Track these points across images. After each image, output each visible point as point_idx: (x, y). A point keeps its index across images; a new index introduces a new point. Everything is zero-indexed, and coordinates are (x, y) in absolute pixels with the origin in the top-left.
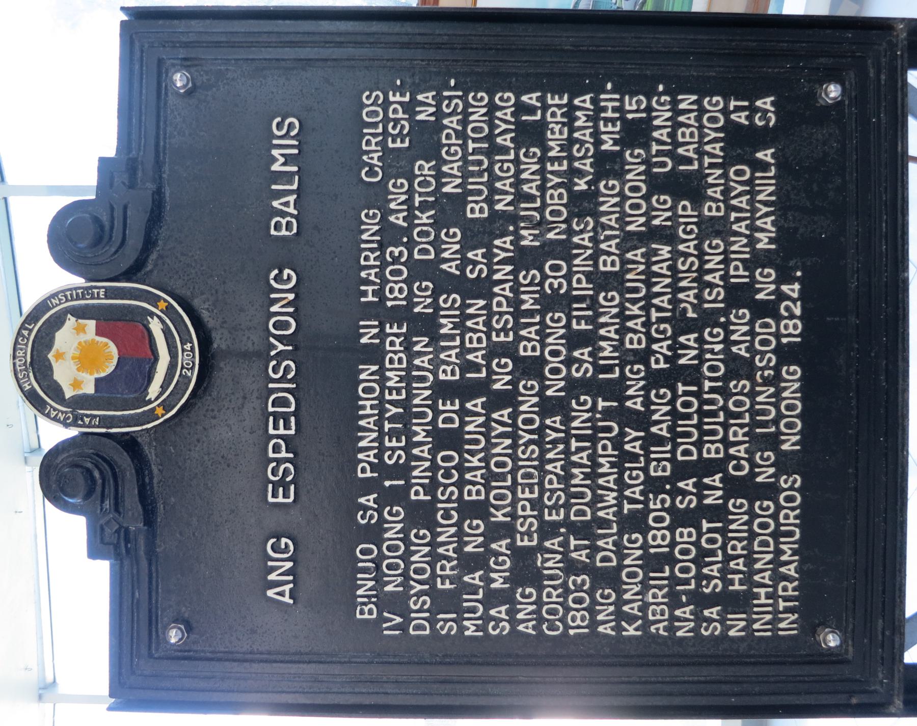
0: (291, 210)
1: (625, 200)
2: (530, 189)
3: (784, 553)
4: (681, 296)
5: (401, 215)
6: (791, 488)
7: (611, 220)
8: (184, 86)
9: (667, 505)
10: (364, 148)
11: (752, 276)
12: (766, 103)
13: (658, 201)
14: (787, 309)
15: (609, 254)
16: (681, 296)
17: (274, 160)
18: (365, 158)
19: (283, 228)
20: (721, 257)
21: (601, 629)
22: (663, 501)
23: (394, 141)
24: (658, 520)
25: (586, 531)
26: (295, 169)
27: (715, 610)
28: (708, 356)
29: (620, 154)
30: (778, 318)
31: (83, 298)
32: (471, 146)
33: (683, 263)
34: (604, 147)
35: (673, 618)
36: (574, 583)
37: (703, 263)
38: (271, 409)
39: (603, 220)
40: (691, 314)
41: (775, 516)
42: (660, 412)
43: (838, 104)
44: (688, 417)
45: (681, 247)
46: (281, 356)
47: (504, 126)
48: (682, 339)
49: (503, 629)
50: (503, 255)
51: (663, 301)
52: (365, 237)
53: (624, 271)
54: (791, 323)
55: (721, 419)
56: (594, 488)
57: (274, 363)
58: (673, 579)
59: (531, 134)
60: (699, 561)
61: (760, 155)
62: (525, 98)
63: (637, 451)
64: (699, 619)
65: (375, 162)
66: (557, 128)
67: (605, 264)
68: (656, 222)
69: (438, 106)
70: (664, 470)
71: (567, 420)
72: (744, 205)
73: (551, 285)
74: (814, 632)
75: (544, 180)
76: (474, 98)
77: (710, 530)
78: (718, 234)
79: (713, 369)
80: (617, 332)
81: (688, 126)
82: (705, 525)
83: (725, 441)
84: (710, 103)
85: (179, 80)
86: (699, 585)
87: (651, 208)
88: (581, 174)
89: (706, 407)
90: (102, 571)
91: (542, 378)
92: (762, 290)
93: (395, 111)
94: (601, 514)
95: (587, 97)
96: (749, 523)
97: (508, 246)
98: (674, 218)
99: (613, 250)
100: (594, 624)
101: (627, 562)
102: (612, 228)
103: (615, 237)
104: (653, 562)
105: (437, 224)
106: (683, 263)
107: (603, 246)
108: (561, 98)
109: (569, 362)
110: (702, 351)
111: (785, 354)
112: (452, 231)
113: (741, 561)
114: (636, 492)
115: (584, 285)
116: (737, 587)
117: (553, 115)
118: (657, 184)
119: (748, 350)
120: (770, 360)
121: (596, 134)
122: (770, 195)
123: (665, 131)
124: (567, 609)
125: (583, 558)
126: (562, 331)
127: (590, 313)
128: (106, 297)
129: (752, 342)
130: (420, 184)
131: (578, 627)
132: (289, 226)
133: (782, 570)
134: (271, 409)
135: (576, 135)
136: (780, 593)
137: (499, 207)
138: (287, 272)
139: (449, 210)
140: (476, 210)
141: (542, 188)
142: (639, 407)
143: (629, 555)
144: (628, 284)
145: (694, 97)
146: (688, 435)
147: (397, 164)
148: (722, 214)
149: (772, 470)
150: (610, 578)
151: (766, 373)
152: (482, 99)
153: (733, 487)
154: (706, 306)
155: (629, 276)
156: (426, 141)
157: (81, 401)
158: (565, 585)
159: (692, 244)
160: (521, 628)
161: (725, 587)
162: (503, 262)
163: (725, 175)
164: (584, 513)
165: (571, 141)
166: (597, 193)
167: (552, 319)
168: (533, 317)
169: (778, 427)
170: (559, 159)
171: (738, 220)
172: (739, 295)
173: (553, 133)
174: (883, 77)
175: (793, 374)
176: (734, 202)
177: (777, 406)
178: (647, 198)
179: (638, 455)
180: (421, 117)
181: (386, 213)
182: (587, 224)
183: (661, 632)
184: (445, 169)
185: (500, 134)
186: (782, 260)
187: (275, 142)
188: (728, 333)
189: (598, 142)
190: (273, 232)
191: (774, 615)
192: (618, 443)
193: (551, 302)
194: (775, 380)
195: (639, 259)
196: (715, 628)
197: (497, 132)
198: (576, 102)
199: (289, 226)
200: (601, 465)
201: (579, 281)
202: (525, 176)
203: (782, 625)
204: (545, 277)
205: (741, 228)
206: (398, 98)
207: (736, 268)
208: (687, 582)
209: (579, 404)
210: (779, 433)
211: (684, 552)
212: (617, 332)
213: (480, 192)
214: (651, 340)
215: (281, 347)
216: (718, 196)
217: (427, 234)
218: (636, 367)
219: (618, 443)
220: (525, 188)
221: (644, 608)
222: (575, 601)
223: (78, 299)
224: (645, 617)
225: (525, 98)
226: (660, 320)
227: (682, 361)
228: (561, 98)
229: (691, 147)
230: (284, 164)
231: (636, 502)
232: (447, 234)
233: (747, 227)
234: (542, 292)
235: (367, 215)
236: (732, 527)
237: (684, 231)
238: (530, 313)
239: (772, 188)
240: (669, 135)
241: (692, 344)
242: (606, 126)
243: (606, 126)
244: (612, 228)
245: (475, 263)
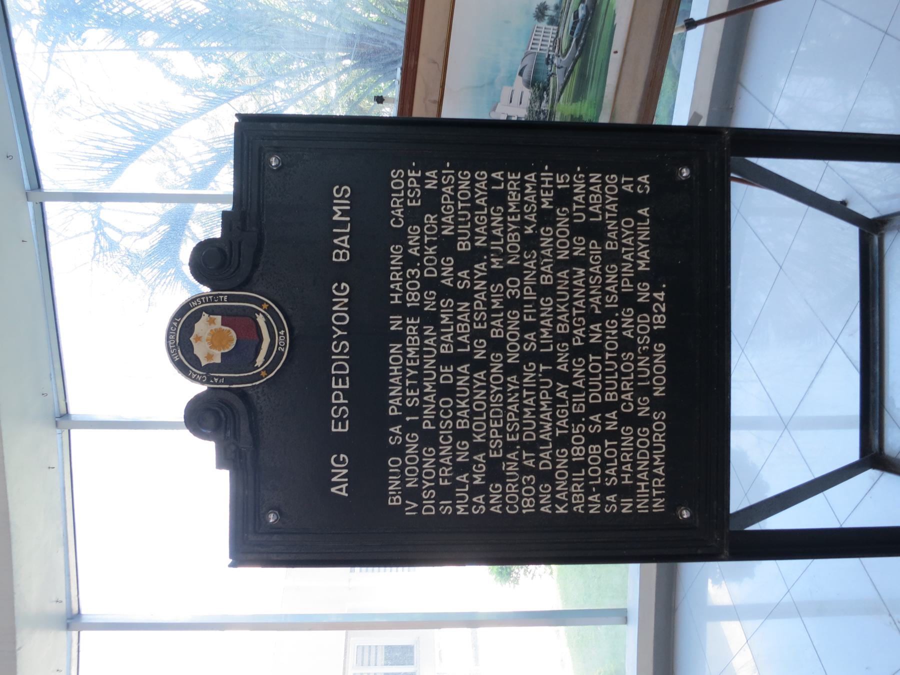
0: (346, 245)
1: (557, 241)
2: (497, 232)
3: (656, 460)
4: (591, 300)
5: (416, 249)
6: (660, 420)
7: (548, 252)
8: (276, 166)
9: (583, 431)
10: (392, 206)
11: (635, 288)
12: (644, 179)
13: (577, 240)
14: (657, 308)
15: (547, 274)
16: (591, 300)
17: (335, 213)
18: (393, 212)
19: (341, 256)
20: (615, 276)
21: (542, 509)
22: (581, 428)
23: (411, 202)
24: (578, 440)
25: (534, 447)
26: (348, 219)
27: (613, 496)
28: (608, 337)
29: (554, 210)
30: (651, 314)
31: (213, 302)
32: (460, 205)
33: (593, 280)
34: (543, 206)
35: (587, 502)
36: (526, 480)
37: (604, 279)
38: (333, 372)
39: (543, 252)
40: (597, 312)
41: (650, 438)
42: (579, 372)
43: (688, 180)
44: (596, 375)
45: (591, 269)
46: (340, 338)
47: (481, 193)
48: (592, 327)
49: (481, 510)
50: (480, 274)
51: (580, 303)
52: (393, 262)
53: (556, 284)
54: (659, 317)
55: (616, 377)
56: (538, 420)
57: (335, 343)
58: (587, 478)
59: (497, 198)
60: (603, 466)
61: (640, 212)
62: (493, 175)
63: (564, 397)
64: (603, 502)
65: (399, 215)
66: (514, 194)
67: (544, 280)
68: (576, 254)
69: (439, 179)
70: (581, 408)
71: (521, 378)
72: (630, 243)
73: (510, 293)
74: (675, 510)
75: (506, 227)
76: (462, 175)
77: (609, 446)
78: (613, 262)
79: (611, 345)
80: (551, 322)
81: (595, 193)
82: (607, 443)
83: (618, 390)
84: (609, 179)
85: (274, 161)
86: (603, 481)
87: (572, 245)
88: (529, 223)
89: (607, 370)
90: (224, 476)
91: (505, 352)
92: (642, 296)
93: (412, 183)
94: (542, 437)
95: (533, 175)
96: (634, 442)
97: (483, 268)
98: (587, 251)
99: (549, 271)
100: (538, 506)
101: (558, 467)
102: (548, 257)
103: (549, 263)
104: (574, 467)
105: (439, 254)
106: (593, 280)
107: (543, 269)
108: (516, 175)
109: (522, 341)
110: (604, 335)
111: (656, 336)
112: (448, 259)
113: (629, 465)
114: (563, 423)
115: (531, 293)
116: (627, 482)
117: (512, 186)
118: (576, 230)
119: (632, 333)
120: (646, 340)
121: (538, 198)
122: (646, 236)
123: (581, 196)
124: (521, 497)
125: (531, 465)
126: (517, 322)
127: (535, 311)
128: (228, 301)
129: (635, 329)
130: (427, 229)
131: (528, 508)
132: (344, 255)
133: (655, 471)
134: (333, 372)
135: (526, 198)
136: (654, 485)
137: (478, 244)
138: (343, 284)
139: (446, 246)
140: (463, 246)
141: (505, 232)
142: (565, 370)
143: (559, 462)
144: (559, 293)
145: (599, 175)
146: (596, 387)
147: (413, 216)
148: (616, 248)
149: (648, 409)
150: (547, 477)
151: (644, 348)
152: (467, 175)
153: (624, 419)
154: (607, 306)
155: (559, 288)
156: (432, 201)
157: (211, 368)
158: (520, 481)
159: (598, 267)
160: (492, 509)
161: (619, 482)
162: (481, 278)
163: (619, 224)
164: (531, 436)
165: (523, 202)
166: (540, 235)
167: (511, 315)
168: (499, 313)
169: (651, 382)
170: (515, 214)
171: (626, 252)
172: (627, 299)
173: (511, 197)
174: (716, 163)
175: (660, 349)
176: (624, 241)
177: (650, 368)
178: (570, 238)
179: (565, 400)
180: (427, 187)
181: (407, 247)
182: (533, 255)
183: (580, 511)
184: (443, 219)
185: (479, 198)
186: (654, 277)
187: (335, 201)
188: (621, 323)
189: (539, 203)
190: (334, 259)
191: (650, 499)
192: (552, 392)
193: (511, 304)
194: (650, 353)
195: (565, 276)
196: (613, 508)
197: (476, 196)
198: (526, 178)
199: (344, 255)
200: (542, 406)
201: (528, 291)
202: (494, 224)
203: (655, 506)
204: (506, 288)
205: (627, 257)
206: (414, 174)
207: (625, 283)
208: (596, 479)
209: (528, 367)
210: (652, 385)
211: (594, 460)
212: (551, 322)
213: (465, 235)
214: (573, 328)
215: (340, 333)
216: (614, 237)
217: (432, 261)
218: (563, 345)
219: (552, 392)
220: (494, 232)
221: (569, 495)
222: (526, 491)
223: (210, 302)
224: (570, 501)
225: (493, 175)
226: (578, 315)
227: (592, 341)
228: (516, 175)
229: (598, 206)
230: (341, 216)
231: (563, 429)
232: (445, 261)
233: (632, 257)
234: (505, 297)
235: (394, 249)
236: (624, 444)
237: (593, 259)
238: (497, 311)
239: (648, 233)
240: (583, 199)
241: (598, 330)
242: (544, 193)
243: (544, 193)
244: (548, 257)
245: (463, 279)
